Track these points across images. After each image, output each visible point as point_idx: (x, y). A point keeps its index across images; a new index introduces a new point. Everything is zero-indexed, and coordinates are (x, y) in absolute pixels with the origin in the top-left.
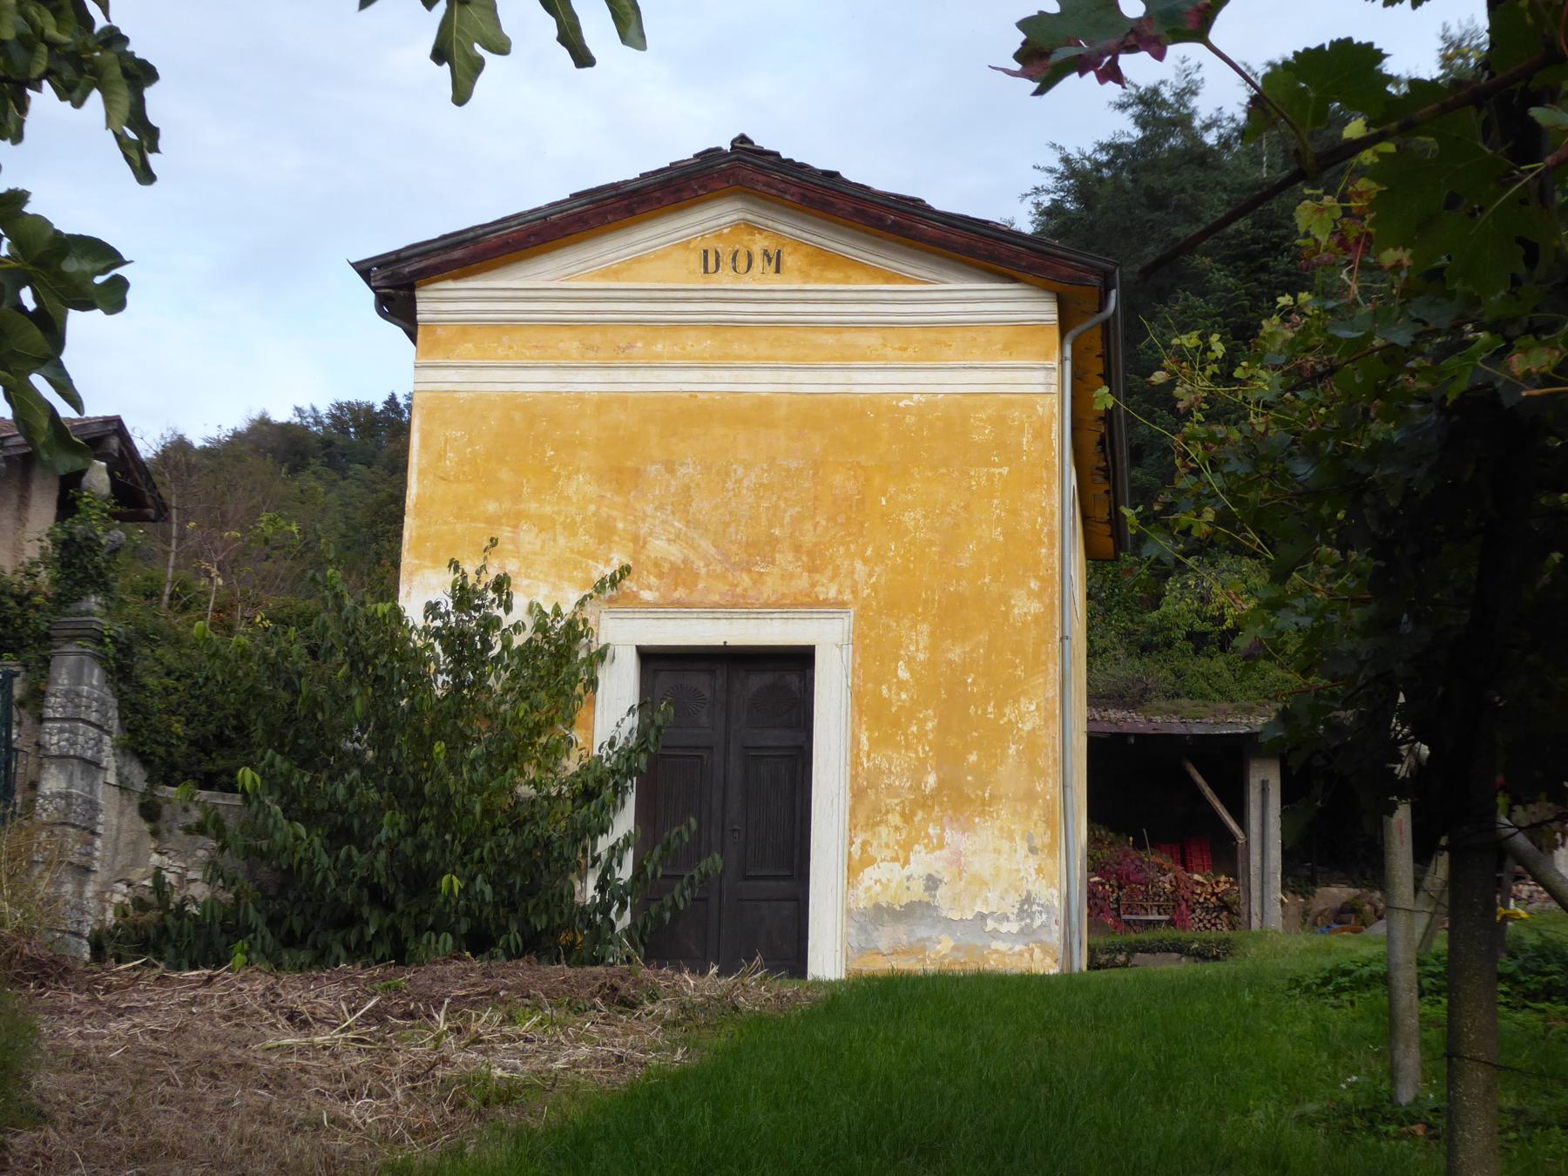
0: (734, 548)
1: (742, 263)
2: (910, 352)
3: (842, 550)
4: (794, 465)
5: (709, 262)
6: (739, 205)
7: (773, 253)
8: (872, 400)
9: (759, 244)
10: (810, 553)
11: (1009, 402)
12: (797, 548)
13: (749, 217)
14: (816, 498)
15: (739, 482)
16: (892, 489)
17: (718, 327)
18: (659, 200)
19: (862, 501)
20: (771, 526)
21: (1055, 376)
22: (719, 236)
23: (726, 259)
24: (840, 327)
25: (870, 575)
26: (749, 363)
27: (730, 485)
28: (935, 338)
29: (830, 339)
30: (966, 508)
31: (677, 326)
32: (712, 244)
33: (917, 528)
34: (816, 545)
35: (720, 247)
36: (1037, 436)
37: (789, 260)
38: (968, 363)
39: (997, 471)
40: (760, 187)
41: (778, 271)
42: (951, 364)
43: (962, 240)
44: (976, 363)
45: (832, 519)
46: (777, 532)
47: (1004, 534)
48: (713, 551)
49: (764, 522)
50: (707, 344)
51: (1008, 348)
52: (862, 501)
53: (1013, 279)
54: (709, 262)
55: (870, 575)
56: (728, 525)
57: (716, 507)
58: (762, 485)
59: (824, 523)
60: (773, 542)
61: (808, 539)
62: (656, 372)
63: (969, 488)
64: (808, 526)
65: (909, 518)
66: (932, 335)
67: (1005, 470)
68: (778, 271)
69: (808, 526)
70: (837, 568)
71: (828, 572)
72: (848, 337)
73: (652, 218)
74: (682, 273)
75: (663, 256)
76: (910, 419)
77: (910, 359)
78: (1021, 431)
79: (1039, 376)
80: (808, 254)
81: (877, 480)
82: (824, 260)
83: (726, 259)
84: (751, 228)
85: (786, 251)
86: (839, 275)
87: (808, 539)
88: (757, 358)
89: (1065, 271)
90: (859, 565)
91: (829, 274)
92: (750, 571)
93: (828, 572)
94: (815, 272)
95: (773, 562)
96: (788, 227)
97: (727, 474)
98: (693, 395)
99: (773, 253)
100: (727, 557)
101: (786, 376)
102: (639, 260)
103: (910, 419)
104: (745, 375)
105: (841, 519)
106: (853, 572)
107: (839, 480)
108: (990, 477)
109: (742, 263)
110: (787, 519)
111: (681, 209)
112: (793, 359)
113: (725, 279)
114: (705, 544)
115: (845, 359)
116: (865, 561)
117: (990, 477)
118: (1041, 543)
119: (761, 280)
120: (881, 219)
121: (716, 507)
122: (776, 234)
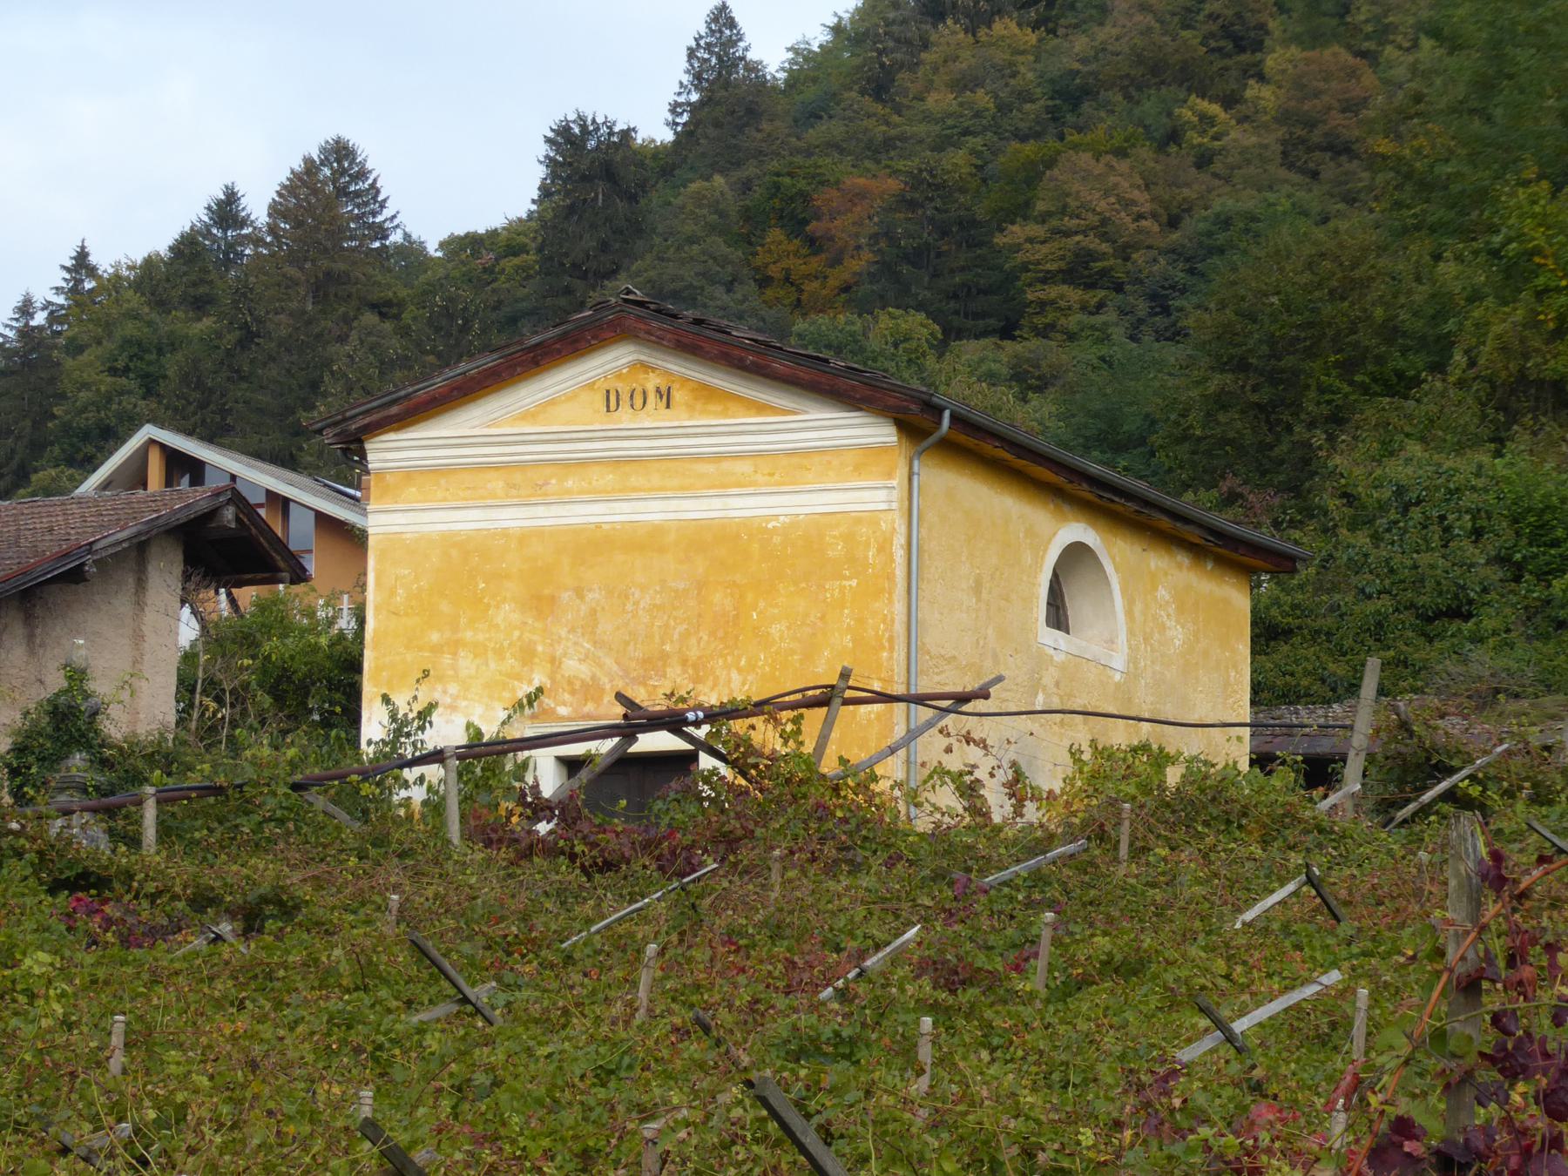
0: (633, 664)
1: (638, 401)
2: (777, 477)
3: (721, 662)
4: (681, 586)
5: (611, 401)
6: (631, 348)
7: (664, 390)
8: (746, 523)
9: (652, 382)
10: (695, 666)
11: (857, 519)
12: (684, 662)
13: (643, 358)
14: (700, 615)
15: (636, 603)
16: (762, 604)
17: (617, 462)
18: (559, 351)
19: (737, 617)
20: (663, 643)
21: (895, 494)
22: (619, 376)
23: (625, 397)
24: (718, 458)
25: (744, 684)
26: (642, 495)
27: (629, 607)
28: (793, 465)
29: (709, 468)
30: (822, 618)
31: (583, 464)
32: (614, 384)
33: (781, 638)
34: (700, 658)
35: (620, 386)
36: (881, 549)
37: (678, 396)
38: (822, 486)
39: (847, 583)
40: (642, 335)
41: (668, 406)
42: (808, 487)
43: (807, 377)
44: (829, 486)
45: (712, 634)
46: (668, 648)
47: (853, 640)
48: (615, 668)
49: (657, 639)
50: (609, 478)
51: (858, 469)
52: (737, 617)
53: (860, 409)
54: (611, 401)
55: (744, 684)
56: (627, 643)
57: (618, 628)
58: (655, 606)
59: (705, 638)
60: (664, 656)
61: (693, 653)
62: (553, 507)
63: (824, 600)
64: (693, 641)
65: (776, 630)
66: (795, 460)
67: (854, 583)
68: (668, 406)
69: (693, 641)
70: (716, 678)
71: (710, 683)
72: (726, 465)
73: (556, 366)
74: (585, 414)
75: (572, 397)
76: (777, 539)
77: (777, 484)
78: (868, 545)
79: (882, 495)
80: (693, 390)
81: (750, 597)
82: (707, 394)
83: (625, 397)
84: (646, 368)
85: (675, 387)
86: (718, 408)
87: (693, 653)
88: (652, 489)
89: (892, 402)
90: (735, 675)
91: (712, 407)
92: (645, 685)
93: (710, 683)
94: (699, 406)
95: (664, 676)
96: (677, 367)
97: (627, 597)
98: (598, 526)
99: (664, 390)
100: (626, 672)
101: (674, 504)
102: (552, 402)
103: (777, 539)
104: (640, 506)
105: (720, 634)
106: (729, 681)
107: (718, 597)
108: (842, 588)
109: (638, 401)
110: (676, 637)
111: (582, 355)
112: (682, 488)
113: (625, 418)
114: (609, 662)
115: (723, 485)
116: (740, 670)
117: (842, 588)
118: (882, 647)
119: (653, 418)
120: (741, 360)
121: (618, 628)
122: (667, 373)
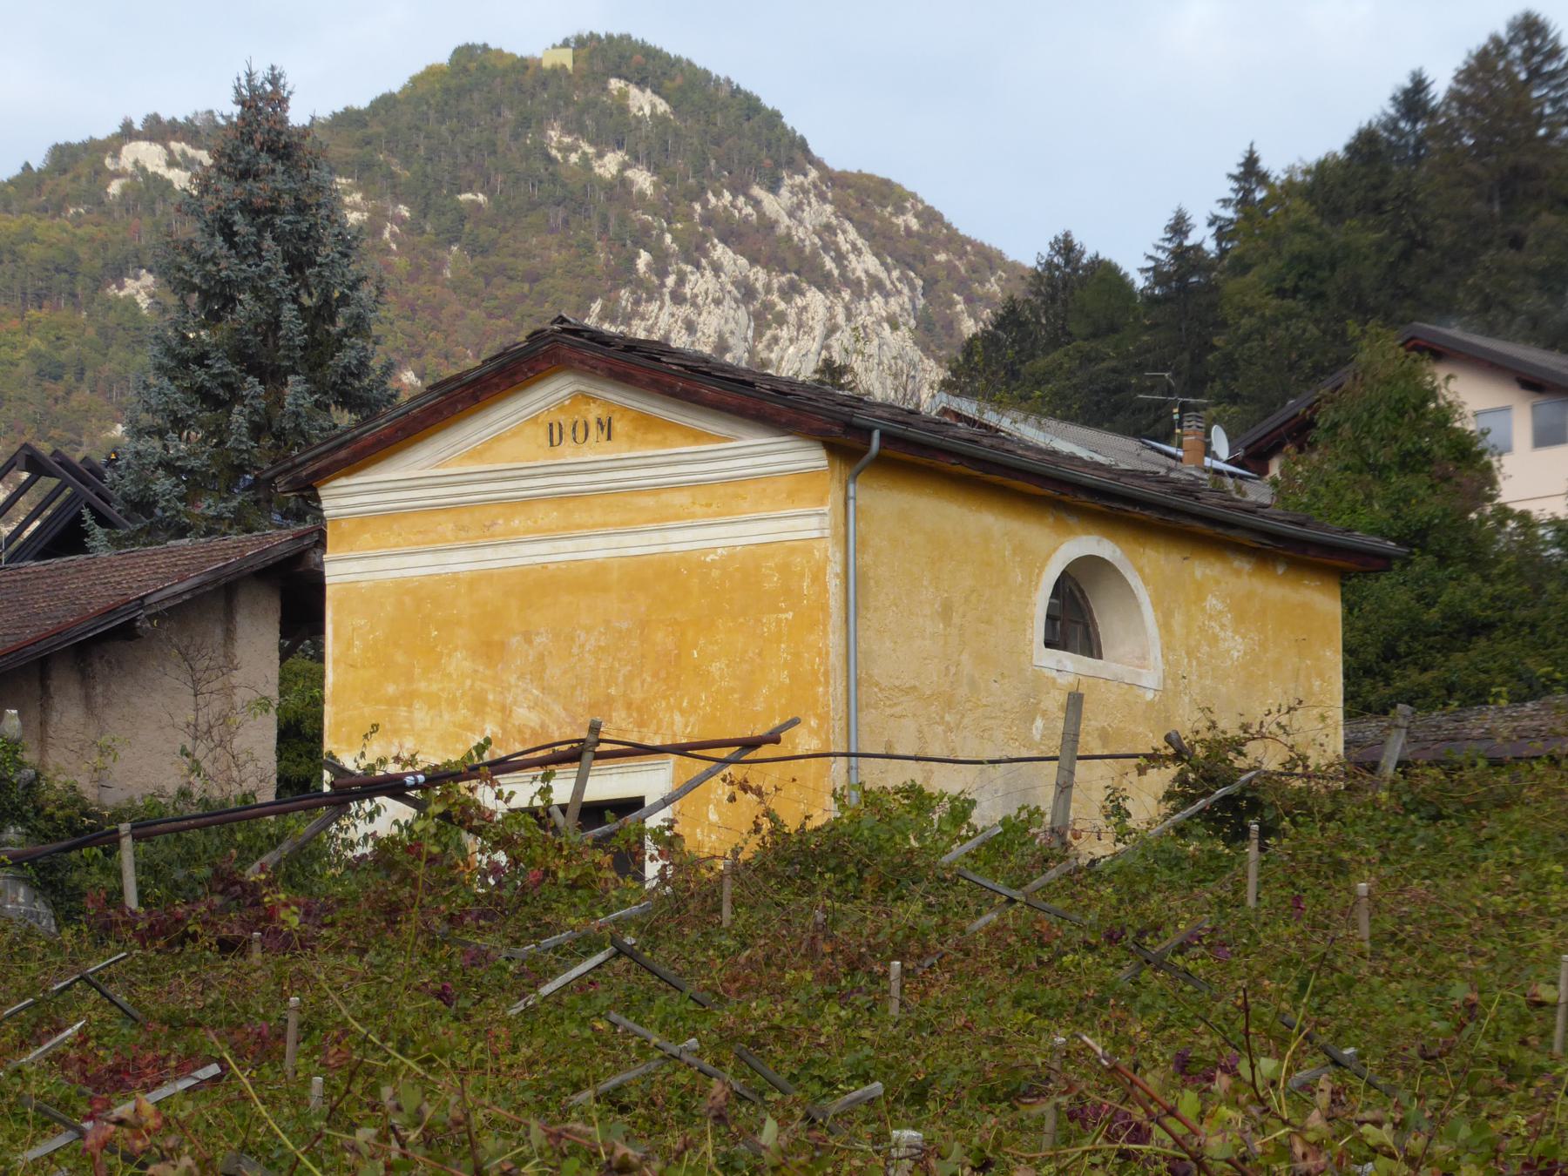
0: (580, 710)
4: (624, 626)
5: (555, 435)
6: (571, 378)
8: (684, 557)
9: (593, 413)
11: (792, 548)
12: (629, 706)
13: (583, 388)
14: (643, 656)
15: (582, 646)
16: (702, 642)
18: (497, 386)
19: (678, 656)
20: (608, 687)
22: (562, 409)
23: (568, 430)
24: (657, 490)
25: (686, 726)
26: (586, 532)
27: (575, 650)
28: (726, 495)
29: (649, 501)
30: (760, 654)
33: (722, 677)
34: (644, 700)
35: (562, 418)
37: (618, 426)
39: (783, 616)
41: (609, 438)
42: (744, 517)
44: (763, 515)
45: (655, 675)
46: (613, 691)
48: (563, 714)
51: (792, 497)
52: (678, 656)
54: (555, 435)
55: (686, 726)
61: (638, 696)
64: (637, 683)
65: (715, 667)
67: (790, 615)
68: (609, 438)
69: (637, 683)
74: (529, 449)
75: (515, 433)
78: (802, 576)
82: (646, 423)
83: (568, 430)
85: (616, 417)
86: (658, 437)
87: (638, 696)
90: (677, 717)
91: (651, 437)
93: (653, 727)
96: (615, 396)
97: (572, 639)
98: (544, 566)
101: (615, 541)
102: (498, 439)
103: (715, 573)
105: (663, 674)
108: (779, 621)
113: (568, 453)
114: (557, 709)
115: (663, 518)
116: (683, 712)
117: (779, 621)
119: (596, 451)
120: (672, 387)
122: (607, 403)
